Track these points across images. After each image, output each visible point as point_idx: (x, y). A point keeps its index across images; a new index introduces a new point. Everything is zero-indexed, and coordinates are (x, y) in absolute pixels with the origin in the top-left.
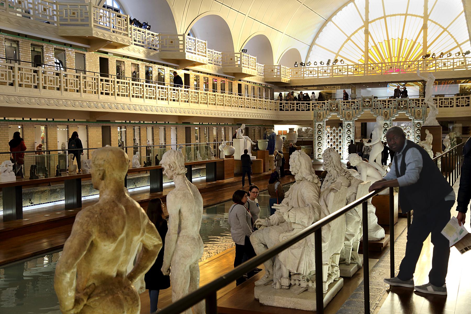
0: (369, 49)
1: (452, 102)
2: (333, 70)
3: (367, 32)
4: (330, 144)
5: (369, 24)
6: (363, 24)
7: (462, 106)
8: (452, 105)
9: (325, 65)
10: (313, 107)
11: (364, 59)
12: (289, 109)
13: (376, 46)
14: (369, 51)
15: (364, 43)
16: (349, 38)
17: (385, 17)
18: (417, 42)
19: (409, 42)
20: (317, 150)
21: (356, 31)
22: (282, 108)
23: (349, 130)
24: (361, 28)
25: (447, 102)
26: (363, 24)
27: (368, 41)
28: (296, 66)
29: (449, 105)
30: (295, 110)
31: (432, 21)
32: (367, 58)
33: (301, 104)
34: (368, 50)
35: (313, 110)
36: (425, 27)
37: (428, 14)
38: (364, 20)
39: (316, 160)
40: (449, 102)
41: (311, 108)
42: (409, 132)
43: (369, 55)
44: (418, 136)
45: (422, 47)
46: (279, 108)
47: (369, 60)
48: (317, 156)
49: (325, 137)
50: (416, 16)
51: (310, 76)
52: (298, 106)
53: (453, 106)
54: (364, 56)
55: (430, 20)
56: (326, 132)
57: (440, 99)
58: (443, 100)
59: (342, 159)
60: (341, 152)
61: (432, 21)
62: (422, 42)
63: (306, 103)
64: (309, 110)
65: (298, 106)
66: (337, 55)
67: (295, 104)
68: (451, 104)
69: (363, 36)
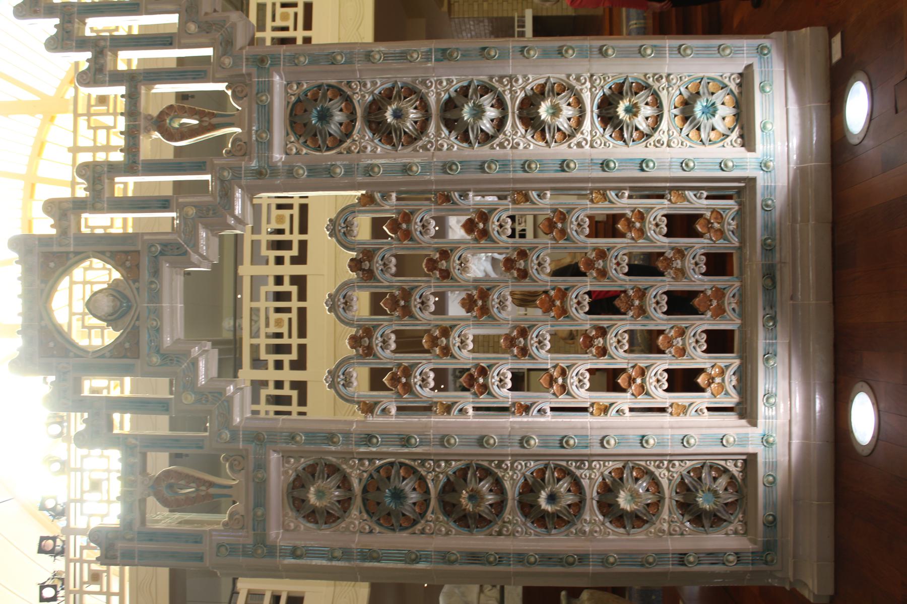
39: (769, 546)
60: (660, 208)
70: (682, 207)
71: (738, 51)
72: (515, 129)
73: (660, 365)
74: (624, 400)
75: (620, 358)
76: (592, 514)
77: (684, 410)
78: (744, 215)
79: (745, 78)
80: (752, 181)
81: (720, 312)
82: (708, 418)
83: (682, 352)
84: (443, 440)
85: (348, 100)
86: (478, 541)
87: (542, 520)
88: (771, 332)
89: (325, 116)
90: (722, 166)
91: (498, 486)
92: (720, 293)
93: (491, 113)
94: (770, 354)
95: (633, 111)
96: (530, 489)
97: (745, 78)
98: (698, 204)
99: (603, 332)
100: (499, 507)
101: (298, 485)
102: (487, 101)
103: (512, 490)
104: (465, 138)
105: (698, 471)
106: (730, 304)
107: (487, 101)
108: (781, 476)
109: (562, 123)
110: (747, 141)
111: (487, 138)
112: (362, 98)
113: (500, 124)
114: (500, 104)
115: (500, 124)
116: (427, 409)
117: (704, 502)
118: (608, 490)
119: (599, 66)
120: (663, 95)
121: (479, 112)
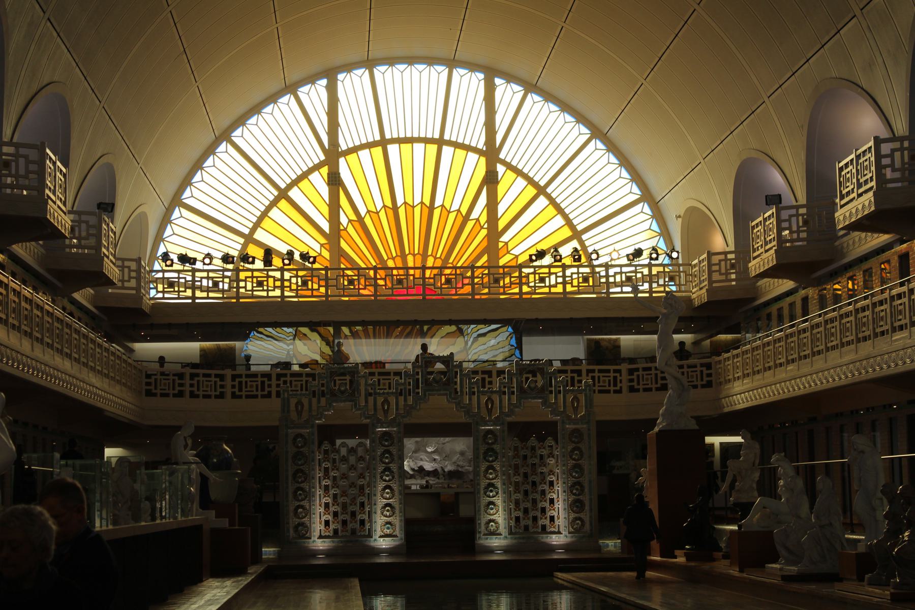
0: (342, 228)
1: (619, 378)
2: (238, 280)
3: (335, 181)
4: (332, 492)
5: (342, 161)
6: (323, 158)
7: (645, 390)
8: (618, 388)
9: (259, 264)
10: (233, 387)
11: (326, 254)
12: (171, 392)
13: (360, 220)
14: (343, 233)
15: (325, 210)
16: (283, 194)
17: (383, 143)
18: (474, 215)
19: (452, 216)
20: (291, 514)
21: (305, 175)
22: (152, 387)
23: (388, 452)
24: (317, 167)
25: (607, 379)
26: (323, 158)
27: (339, 206)
28: (169, 263)
29: (612, 388)
30: (187, 394)
31: (509, 166)
32: (338, 253)
33: (201, 378)
34: (339, 230)
35: (278, 394)
36: (491, 180)
37: (498, 145)
38: (327, 146)
40: (612, 379)
41: (228, 391)
42: (551, 455)
43: (343, 244)
44: (577, 467)
45: (484, 232)
46: (145, 387)
47: (343, 260)
48: (291, 531)
49: (319, 474)
50: (468, 148)
51: (211, 295)
52: (195, 382)
53: (619, 391)
54: (327, 246)
55: (503, 162)
56: (319, 456)
57: (588, 371)
58: (596, 374)
59: (370, 535)
60: (366, 517)
61: (509, 166)
62: (483, 219)
63: (216, 376)
64: (221, 396)
65: (195, 382)
66: (249, 239)
67: (188, 376)
68: (615, 385)
69: (325, 190)
70: (366, 522)
71: (401, 534)
72: (383, 484)
73: (330, 518)
74: (322, 510)
75: (332, 509)
76: (297, 504)
77: (320, 523)
78: (365, 536)
79: (395, 536)
80: (372, 537)
81: (342, 531)
82: (319, 529)
83: (334, 523)
84: (313, 470)
85: (391, 445)
86: (290, 478)
87: (295, 492)
88: (338, 542)
89: (386, 440)
90: (375, 531)
91: (302, 482)
92: (347, 531)
93: (387, 478)
94: (333, 542)
95: (388, 511)
96: (302, 489)
97: (395, 536)
98: (367, 526)
99: (338, 505)
100: (298, 482)
101: (301, 436)
102: (391, 477)
103: (302, 485)
104: (382, 472)
105: (307, 527)
106: (344, 533)
107: (391, 477)
108: (306, 545)
109: (385, 495)
110: (381, 537)
111: (381, 478)
112: (391, 449)
113: (385, 481)
114: (389, 481)
115: (385, 481)
116: (320, 465)
117: (300, 528)
118: (302, 507)
119: (398, 503)
120: (392, 518)
121: (387, 476)
